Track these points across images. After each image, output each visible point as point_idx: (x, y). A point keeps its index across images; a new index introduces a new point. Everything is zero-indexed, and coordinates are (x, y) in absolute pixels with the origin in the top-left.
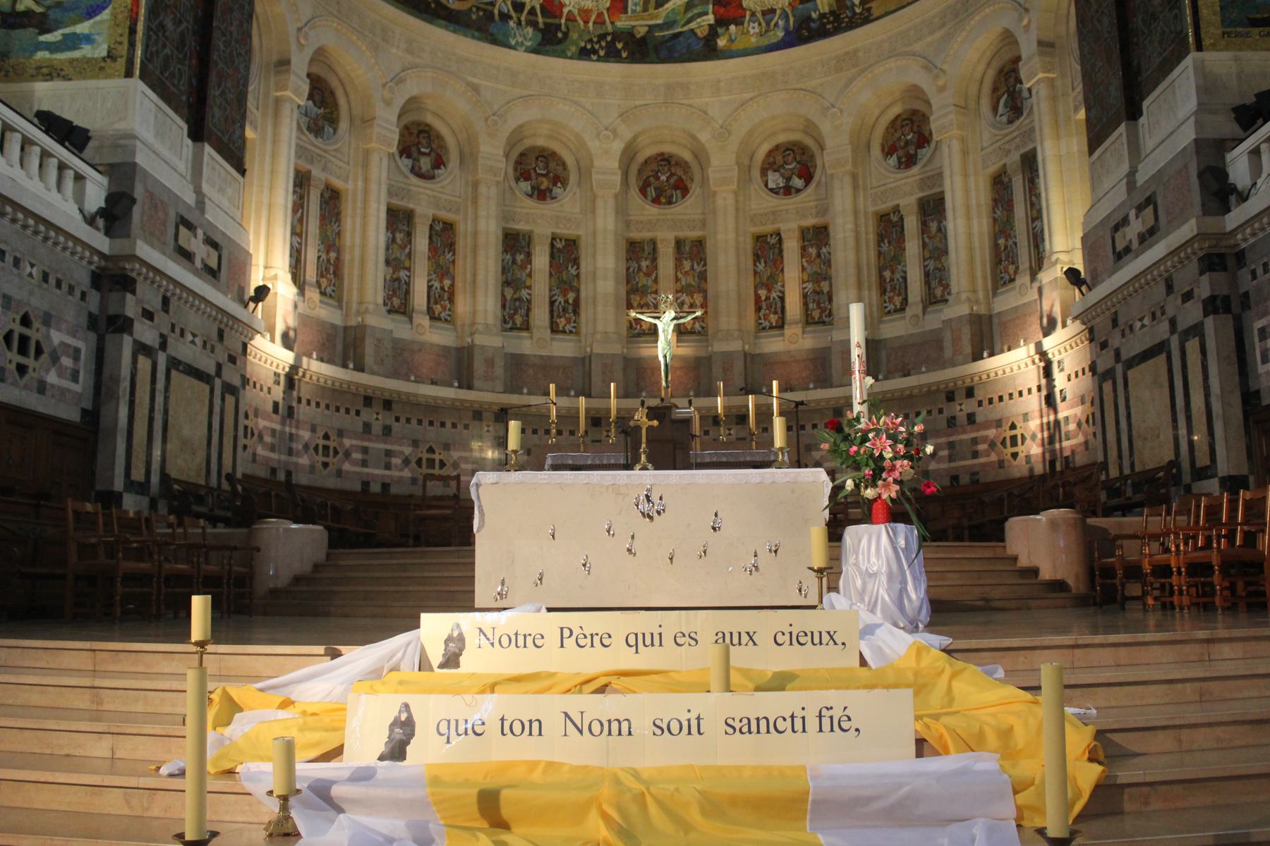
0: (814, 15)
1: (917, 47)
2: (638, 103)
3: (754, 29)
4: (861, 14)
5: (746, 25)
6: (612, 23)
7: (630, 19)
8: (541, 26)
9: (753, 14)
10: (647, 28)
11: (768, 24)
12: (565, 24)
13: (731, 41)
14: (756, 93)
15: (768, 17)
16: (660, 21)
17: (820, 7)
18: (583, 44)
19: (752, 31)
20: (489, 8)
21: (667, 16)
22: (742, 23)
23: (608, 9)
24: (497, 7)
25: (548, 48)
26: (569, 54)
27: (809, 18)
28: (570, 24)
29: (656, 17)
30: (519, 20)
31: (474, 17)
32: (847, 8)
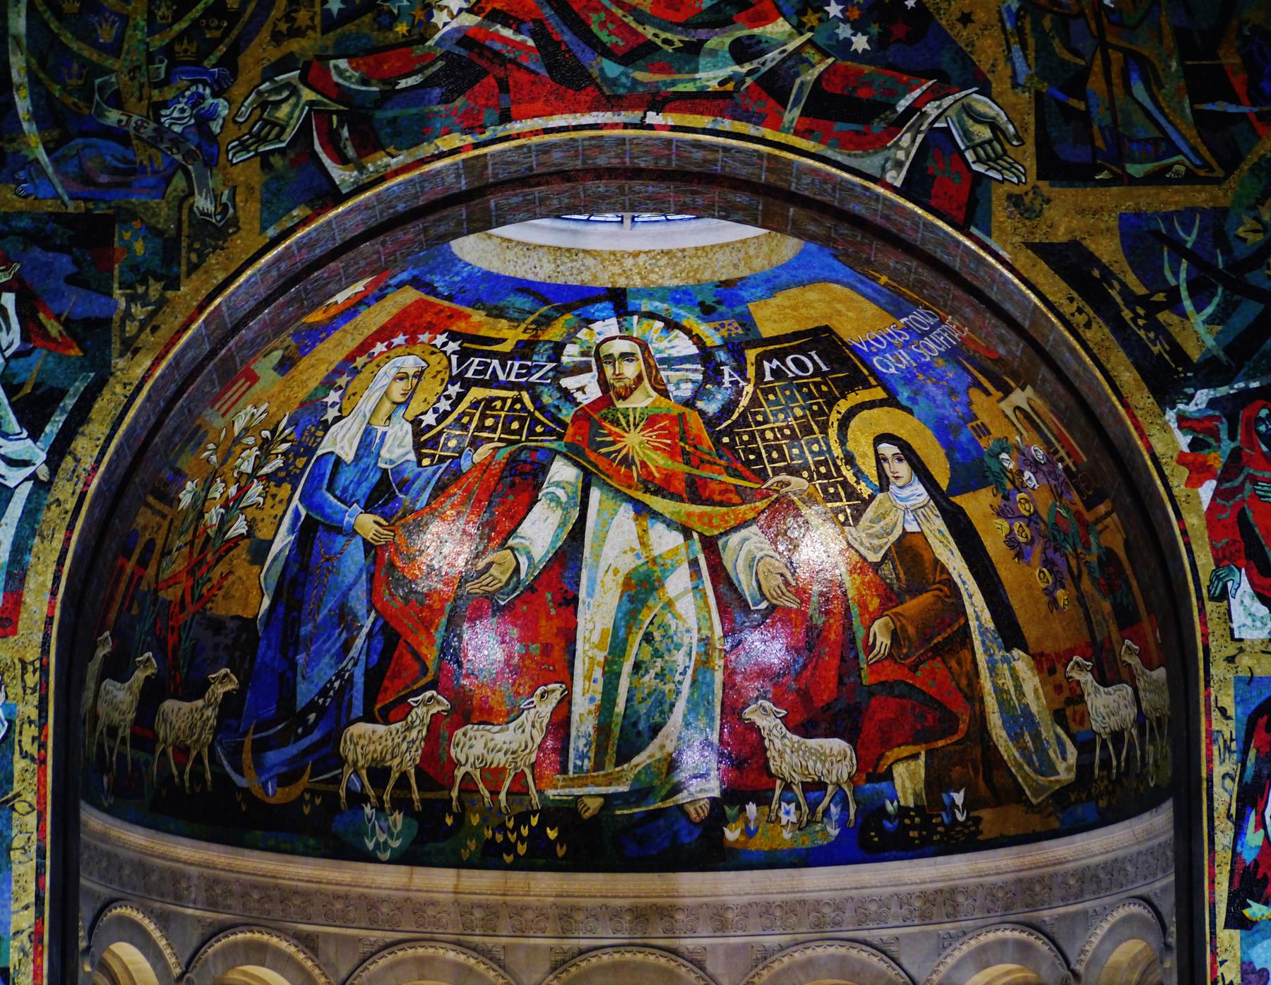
0: (890, 808)
1: (1046, 915)
2: (585, 943)
3: (788, 814)
4: (963, 824)
5: (774, 806)
6: (540, 792)
7: (572, 783)
8: (417, 806)
9: (788, 787)
10: (601, 800)
11: (813, 807)
12: (459, 798)
13: (748, 833)
14: (788, 938)
15: (814, 795)
16: (624, 788)
17: (900, 794)
18: (488, 834)
19: (784, 819)
20: (331, 787)
21: (637, 778)
22: (768, 802)
23: (533, 766)
24: (344, 785)
25: (431, 846)
26: (465, 855)
27: (883, 807)
28: (465, 796)
29: (618, 780)
30: (380, 799)
31: (307, 810)
32: (944, 808)
